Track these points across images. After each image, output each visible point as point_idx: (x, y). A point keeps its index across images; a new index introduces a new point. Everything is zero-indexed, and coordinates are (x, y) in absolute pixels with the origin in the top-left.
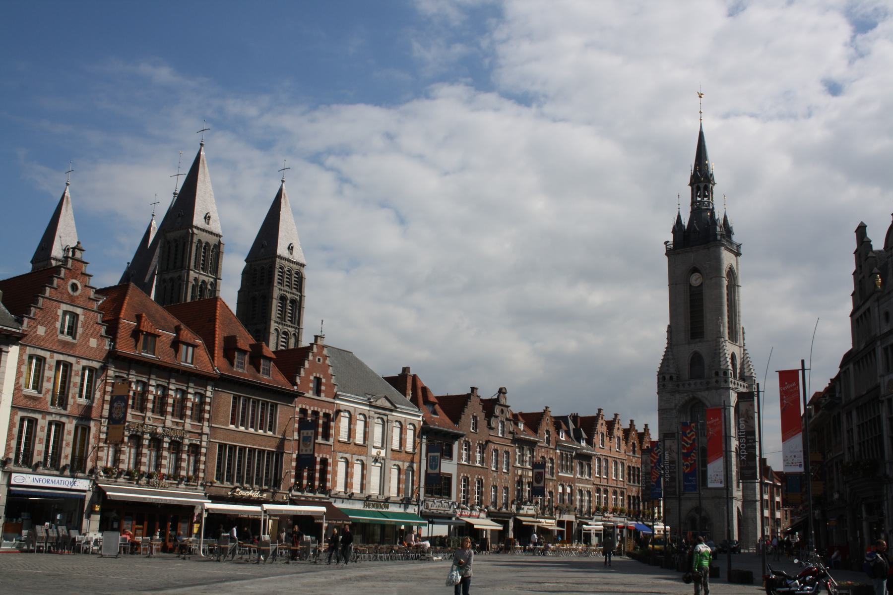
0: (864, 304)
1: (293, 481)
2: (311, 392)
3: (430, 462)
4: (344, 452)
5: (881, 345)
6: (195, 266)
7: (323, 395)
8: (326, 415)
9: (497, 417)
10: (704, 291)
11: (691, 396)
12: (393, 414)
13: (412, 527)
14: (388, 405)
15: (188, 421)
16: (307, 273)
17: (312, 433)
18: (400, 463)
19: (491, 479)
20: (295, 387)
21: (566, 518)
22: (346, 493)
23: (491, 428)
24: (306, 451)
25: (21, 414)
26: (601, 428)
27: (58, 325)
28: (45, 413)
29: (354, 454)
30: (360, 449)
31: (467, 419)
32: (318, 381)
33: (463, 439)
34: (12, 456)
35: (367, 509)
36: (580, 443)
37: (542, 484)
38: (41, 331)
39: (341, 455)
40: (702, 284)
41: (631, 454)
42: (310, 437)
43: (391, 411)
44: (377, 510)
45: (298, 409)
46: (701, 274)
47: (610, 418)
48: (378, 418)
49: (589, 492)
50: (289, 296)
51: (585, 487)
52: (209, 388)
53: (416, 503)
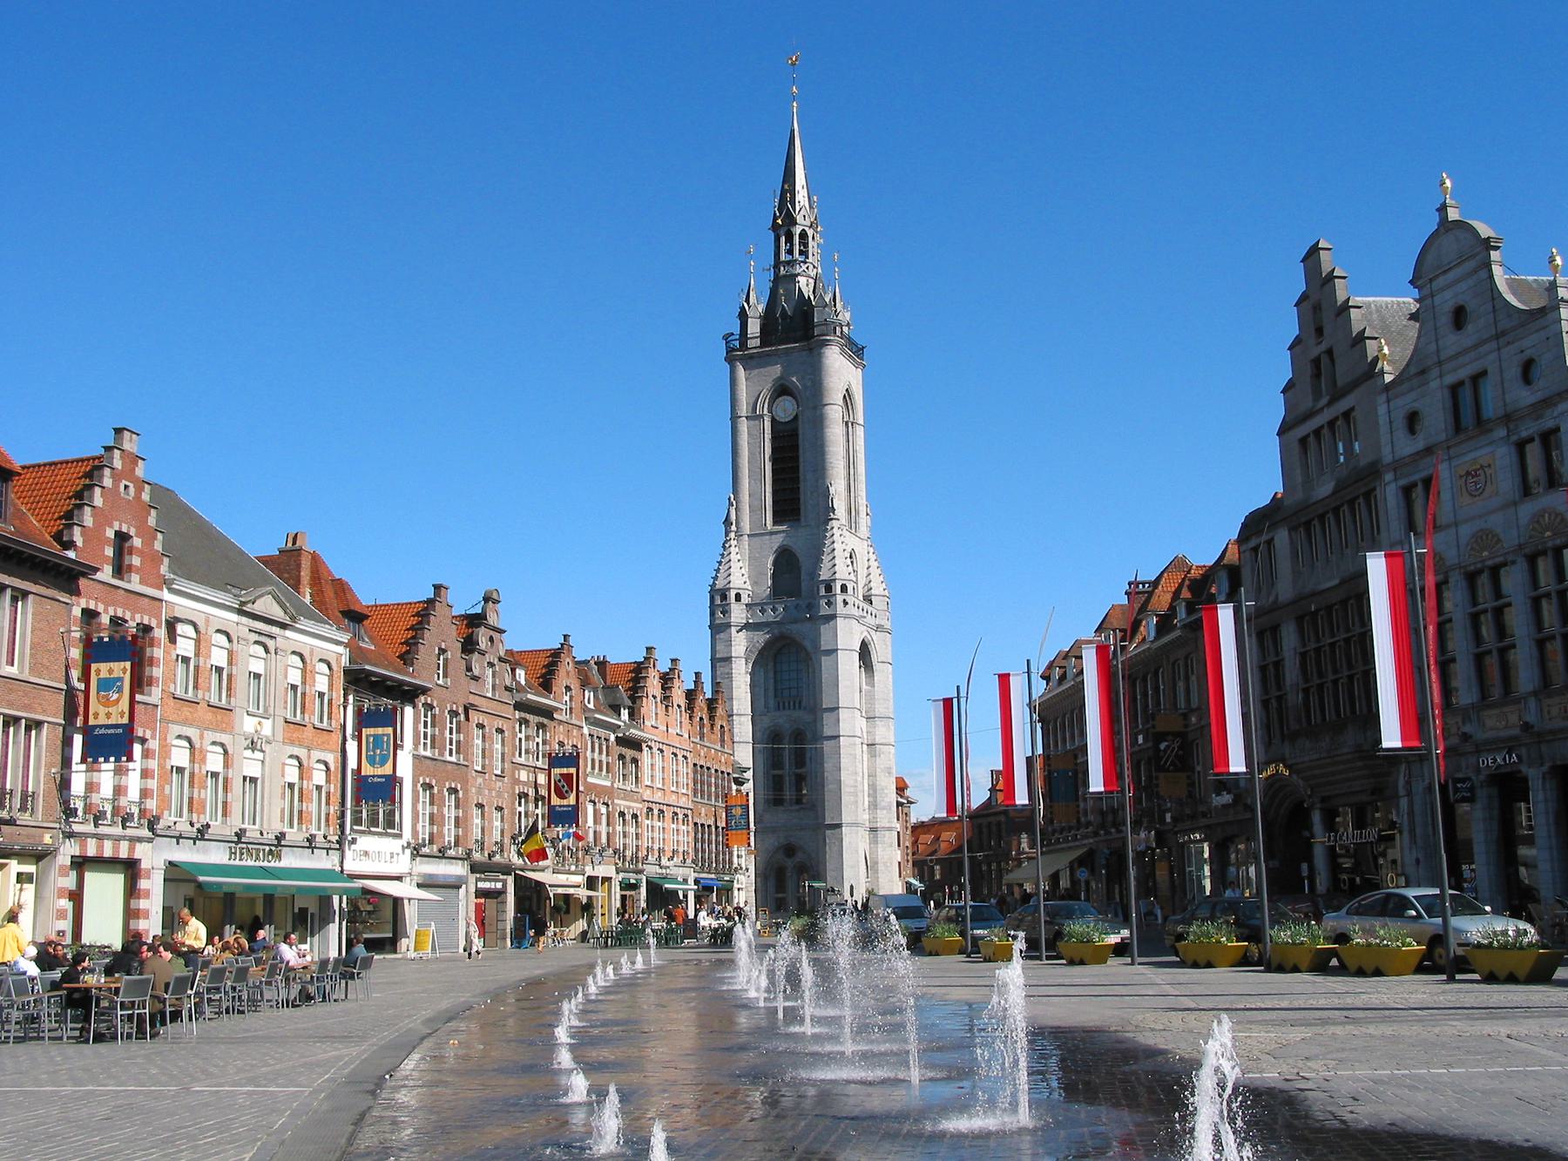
0: (1330, 404)
3: (367, 751)
5: (1396, 480)
7: (135, 578)
8: (147, 629)
9: (483, 653)
10: (800, 432)
11: (776, 631)
12: (288, 633)
13: (329, 898)
17: (124, 671)
18: (302, 752)
19: (474, 790)
20: (71, 554)
21: (602, 871)
22: (192, 824)
23: (476, 678)
24: (108, 715)
26: (653, 686)
29: (207, 729)
30: (219, 717)
31: (426, 652)
33: (422, 698)
35: (237, 862)
36: (620, 715)
37: (572, 800)
39: (176, 729)
40: (796, 418)
41: (697, 740)
42: (121, 679)
43: (283, 626)
44: (257, 864)
45: (77, 612)
46: (797, 401)
47: (664, 666)
48: (256, 642)
49: (635, 816)
51: (629, 808)
53: (338, 846)
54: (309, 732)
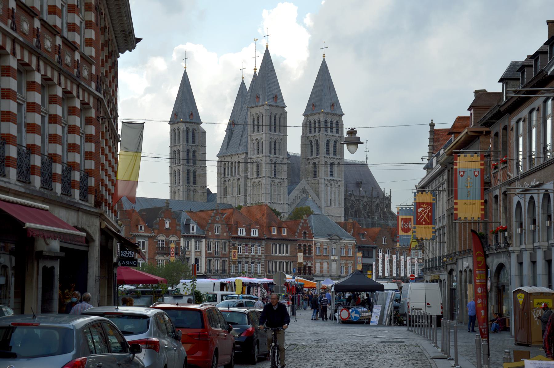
1: (297, 271)
2: (302, 238)
4: (319, 259)
8: (310, 246)
12: (341, 241)
14: (337, 238)
20: (296, 237)
25: (208, 259)
27: (215, 231)
28: (214, 258)
32: (305, 233)
34: (207, 271)
38: (210, 233)
45: (297, 245)
52: (263, 242)
54: (347, 258)
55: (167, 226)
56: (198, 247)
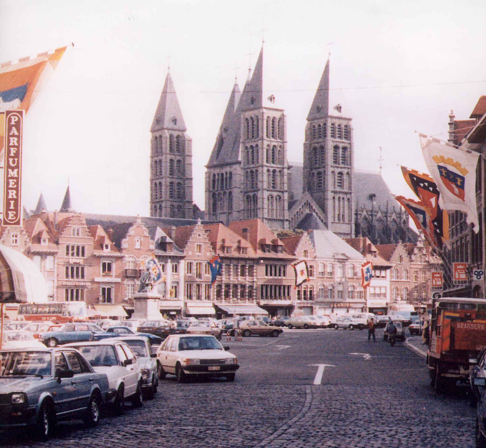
6: (267, 136)
7: (309, 257)
9: (415, 254)
15: (247, 277)
16: (352, 124)
25: (187, 283)
43: (347, 260)
50: (341, 145)
55: (138, 246)
56: (175, 269)
